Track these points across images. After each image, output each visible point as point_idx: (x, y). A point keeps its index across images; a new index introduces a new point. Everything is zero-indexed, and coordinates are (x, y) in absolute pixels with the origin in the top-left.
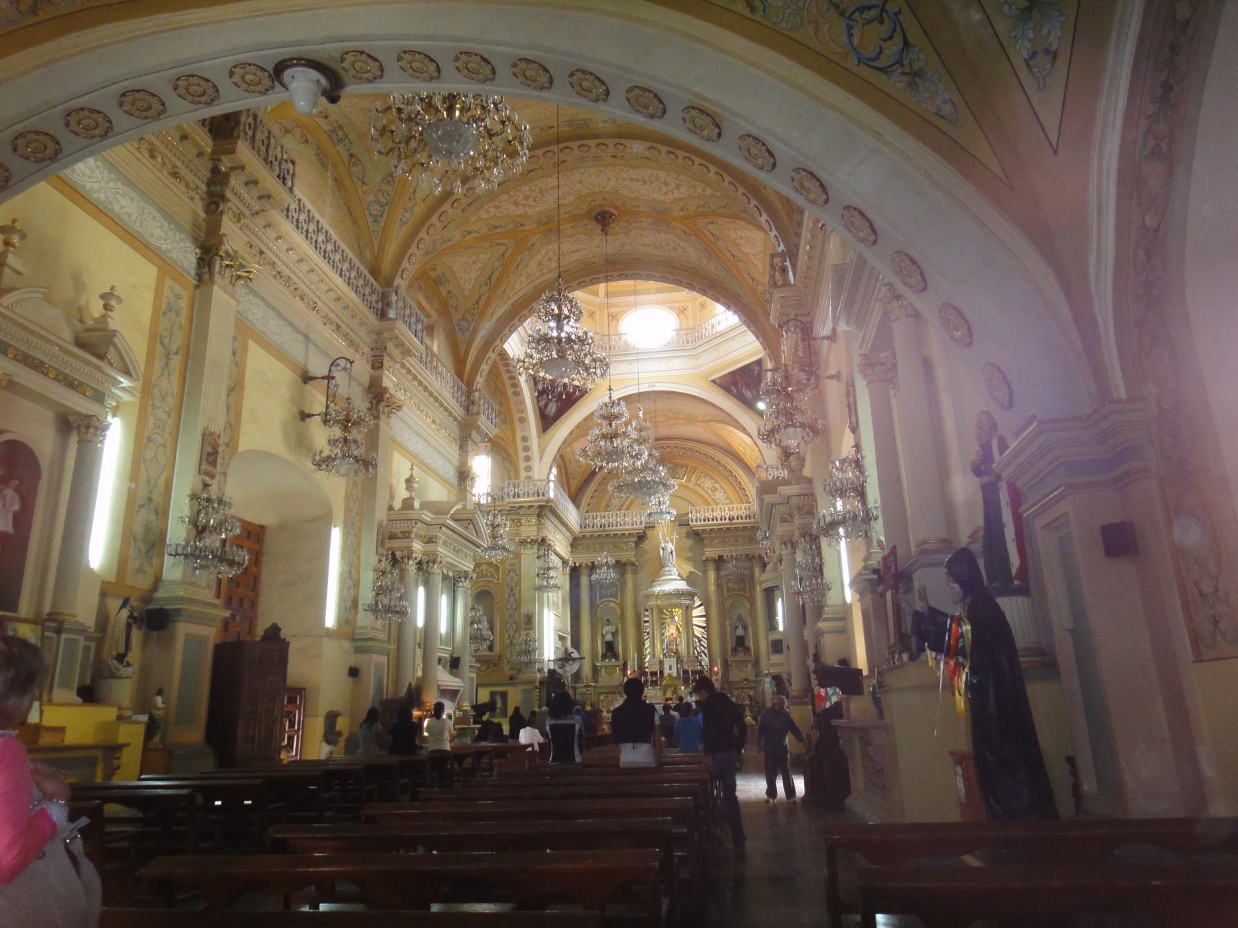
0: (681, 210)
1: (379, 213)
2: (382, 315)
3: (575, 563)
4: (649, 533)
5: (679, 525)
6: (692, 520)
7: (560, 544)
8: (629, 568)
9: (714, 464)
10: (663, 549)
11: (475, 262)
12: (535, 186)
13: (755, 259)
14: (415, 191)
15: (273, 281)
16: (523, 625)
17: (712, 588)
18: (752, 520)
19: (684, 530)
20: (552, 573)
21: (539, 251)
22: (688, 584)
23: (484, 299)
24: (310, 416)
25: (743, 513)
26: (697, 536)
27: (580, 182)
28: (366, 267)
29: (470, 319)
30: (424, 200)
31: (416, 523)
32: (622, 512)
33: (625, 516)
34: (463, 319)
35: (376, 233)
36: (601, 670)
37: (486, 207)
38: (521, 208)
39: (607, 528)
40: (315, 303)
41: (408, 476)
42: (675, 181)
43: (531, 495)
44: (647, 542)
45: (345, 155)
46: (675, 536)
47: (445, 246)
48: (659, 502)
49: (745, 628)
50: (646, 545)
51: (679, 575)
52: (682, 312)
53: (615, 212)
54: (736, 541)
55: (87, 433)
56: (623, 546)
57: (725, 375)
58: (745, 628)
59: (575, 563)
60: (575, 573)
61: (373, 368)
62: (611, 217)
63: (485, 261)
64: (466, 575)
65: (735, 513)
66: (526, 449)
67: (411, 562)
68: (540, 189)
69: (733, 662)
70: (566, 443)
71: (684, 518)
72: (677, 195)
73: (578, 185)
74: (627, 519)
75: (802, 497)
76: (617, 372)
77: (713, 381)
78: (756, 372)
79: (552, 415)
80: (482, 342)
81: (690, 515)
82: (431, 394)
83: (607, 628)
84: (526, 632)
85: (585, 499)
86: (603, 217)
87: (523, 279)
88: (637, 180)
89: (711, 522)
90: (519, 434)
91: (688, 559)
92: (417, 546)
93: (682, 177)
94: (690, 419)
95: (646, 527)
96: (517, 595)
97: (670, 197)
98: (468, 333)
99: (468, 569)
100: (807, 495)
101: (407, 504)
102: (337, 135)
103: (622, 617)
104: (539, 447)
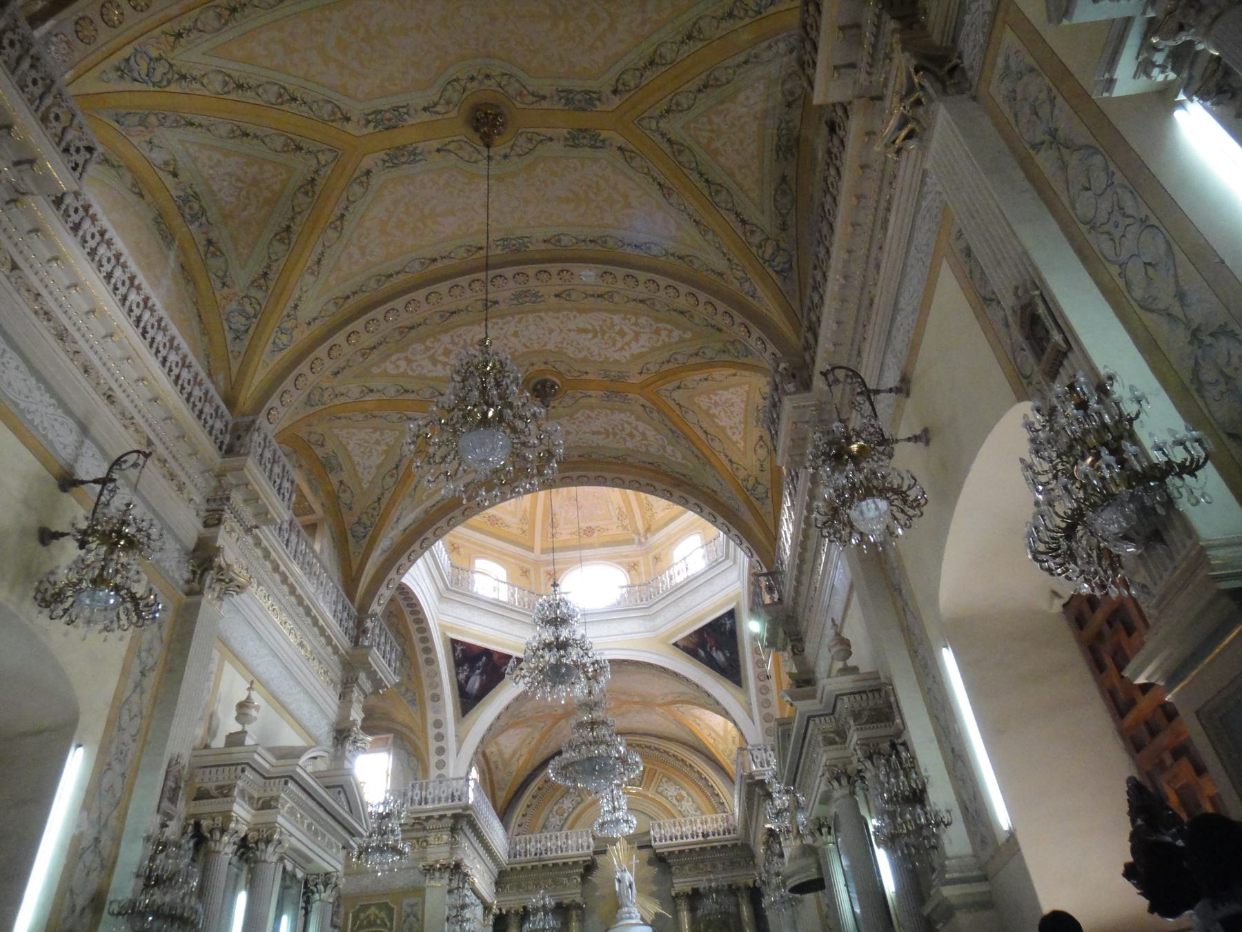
0: (641, 373)
1: (243, 328)
2: (229, 451)
3: (500, 910)
4: (600, 860)
5: (640, 848)
6: (655, 841)
7: (481, 877)
9: (678, 764)
10: (619, 881)
11: (378, 443)
12: (460, 336)
13: (734, 434)
14: (296, 306)
15: (33, 316)
18: (733, 835)
19: (646, 853)
20: (467, 914)
24: (58, 535)
25: (721, 825)
26: (662, 862)
27: (515, 334)
28: (219, 394)
29: (368, 523)
30: (309, 324)
31: (243, 771)
32: (564, 832)
33: (567, 838)
34: (358, 523)
35: (236, 354)
37: (394, 358)
38: (439, 367)
39: (544, 856)
40: (110, 389)
41: (243, 698)
42: (633, 327)
43: (443, 800)
44: (596, 873)
45: (201, 240)
46: (634, 861)
47: (336, 401)
48: (614, 808)
50: (596, 877)
51: (642, 919)
52: (632, 568)
53: (558, 381)
59: (500, 910)
61: (206, 525)
62: (552, 387)
63: (392, 443)
64: (327, 880)
65: (710, 827)
66: (440, 737)
67: (226, 838)
68: (465, 340)
70: (493, 732)
71: (646, 838)
72: (636, 349)
73: (514, 340)
74: (570, 842)
75: (858, 697)
77: (675, 644)
78: (728, 626)
80: (383, 557)
81: (652, 833)
82: (300, 602)
85: (516, 818)
86: (544, 386)
88: (585, 331)
89: (680, 841)
90: (431, 717)
91: (653, 895)
92: (242, 813)
93: (642, 320)
94: (646, 703)
95: (596, 853)
97: (627, 354)
98: (364, 543)
99: (331, 869)
100: (864, 692)
101: (235, 740)
102: (191, 208)
104: (456, 736)
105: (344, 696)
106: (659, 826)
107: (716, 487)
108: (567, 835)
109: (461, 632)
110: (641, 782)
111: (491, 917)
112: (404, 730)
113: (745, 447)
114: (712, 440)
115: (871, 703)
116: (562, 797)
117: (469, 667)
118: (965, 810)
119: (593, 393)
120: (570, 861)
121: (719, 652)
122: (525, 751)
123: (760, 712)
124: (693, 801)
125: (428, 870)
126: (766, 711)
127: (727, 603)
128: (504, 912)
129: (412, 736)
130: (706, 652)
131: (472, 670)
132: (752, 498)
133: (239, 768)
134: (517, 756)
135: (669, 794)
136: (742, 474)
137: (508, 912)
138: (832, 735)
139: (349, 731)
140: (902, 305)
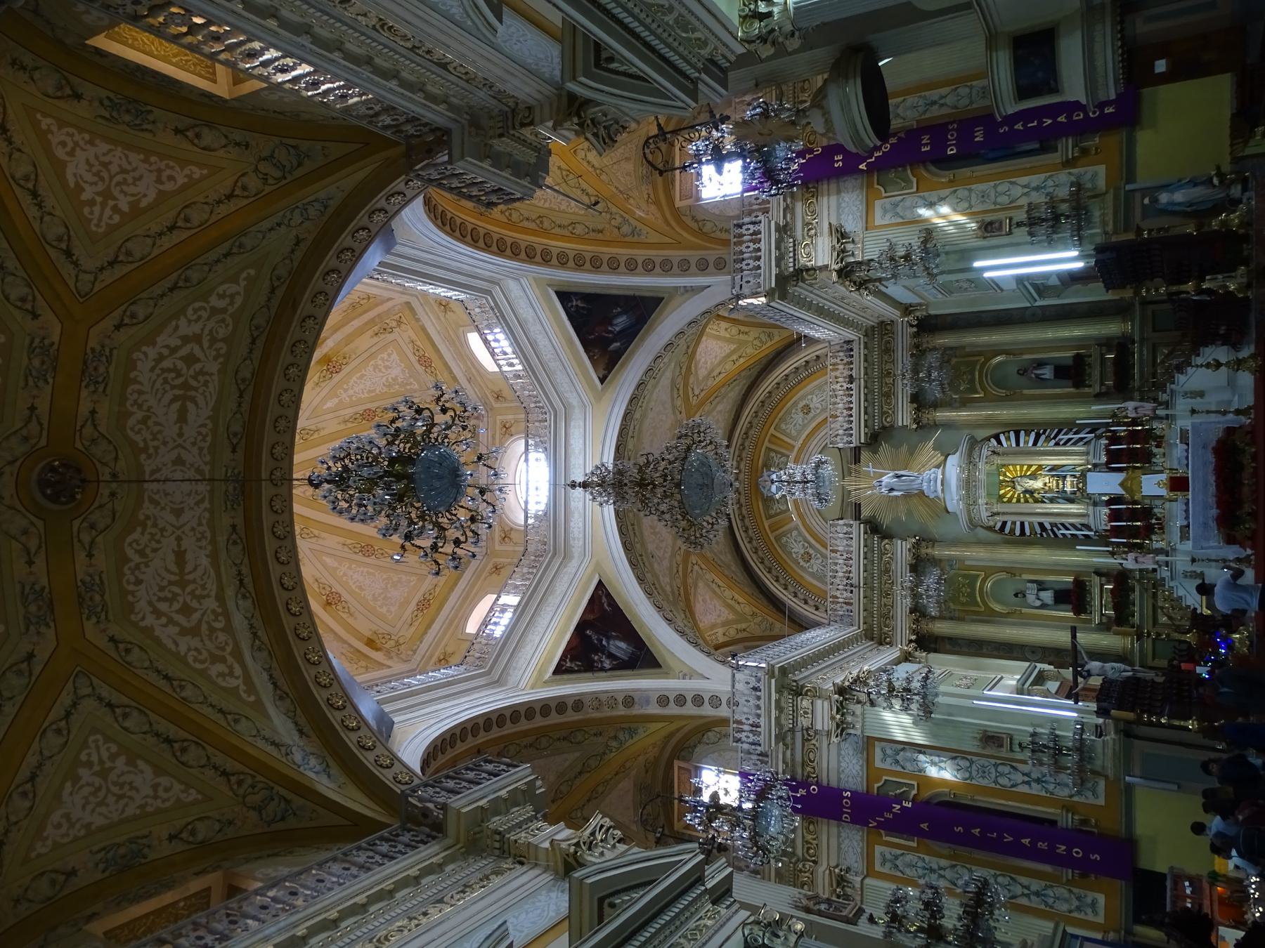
3: (911, 641)
6: (851, 442)
8: (923, 551)
10: (892, 490)
16: (1004, 753)
17: (963, 415)
19: (865, 455)
21: (148, 631)
22: (954, 454)
23: (219, 759)
33: (836, 551)
34: (259, 809)
49: (1041, 364)
50: (886, 520)
51: (938, 467)
52: (507, 430)
56: (885, 558)
59: (911, 641)
60: (927, 643)
62: (53, 470)
66: (681, 700)
69: (1102, 384)
74: (840, 548)
76: (581, 535)
77: (602, 380)
79: (631, 649)
81: (840, 445)
83: (1031, 598)
84: (1017, 748)
85: (807, 611)
90: (654, 709)
91: (912, 452)
95: (857, 517)
98: (298, 801)
103: (1011, 571)
105: (523, 857)
108: (832, 551)
109: (549, 661)
110: (783, 455)
111: (917, 654)
112: (669, 748)
119: (84, 409)
121: (615, 322)
122: (728, 593)
123: (695, 275)
125: (842, 731)
126: (693, 268)
127: (548, 299)
128: (913, 637)
129: (679, 736)
130: (614, 341)
131: (602, 649)
135: (800, 422)
137: (914, 632)
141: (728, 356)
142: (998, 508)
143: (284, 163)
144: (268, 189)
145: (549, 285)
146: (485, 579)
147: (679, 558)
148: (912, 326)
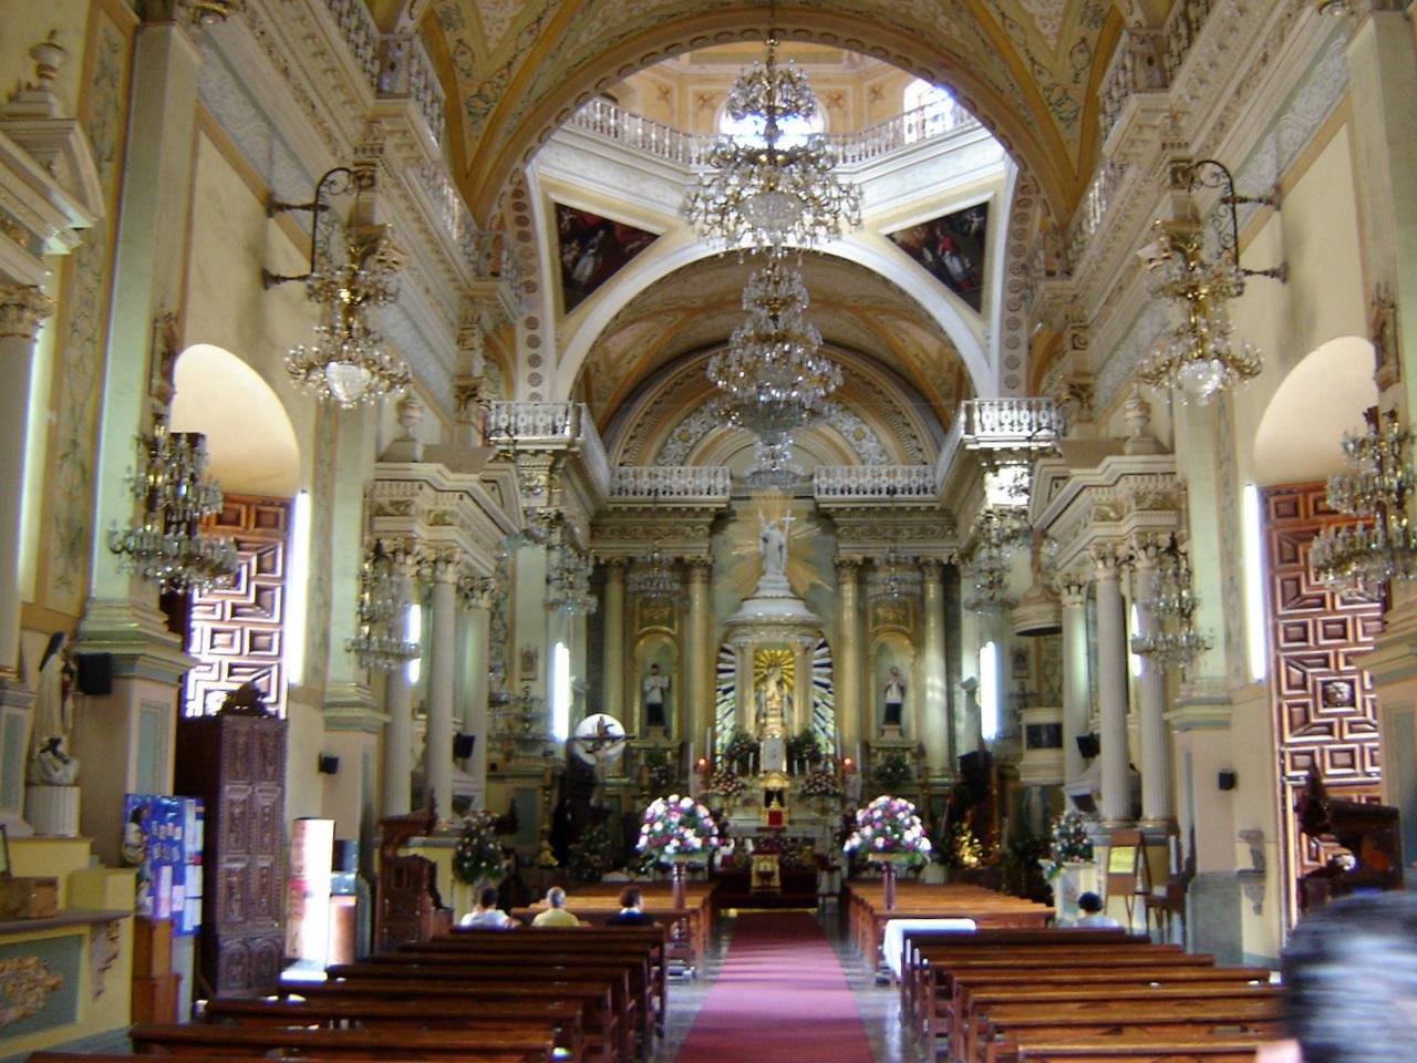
6: (819, 490)
10: (766, 540)
13: (1045, 26)
18: (929, 496)
22: (807, 607)
23: (522, 57)
24: (279, 279)
26: (824, 517)
29: (492, 95)
32: (688, 468)
34: (479, 95)
36: (637, 756)
39: (661, 497)
49: (902, 690)
51: (792, 589)
54: (897, 532)
55: (20, 320)
57: (915, 228)
58: (902, 690)
65: (900, 481)
66: (534, 342)
69: (879, 749)
70: (606, 334)
71: (806, 484)
75: (1146, 477)
77: (890, 237)
79: (584, 279)
81: (815, 481)
83: (650, 682)
85: (621, 444)
87: (596, 24)
92: (421, 530)
95: (733, 498)
96: (507, 617)
98: (484, 123)
103: (681, 664)
104: (557, 340)
106: (828, 471)
107: (1005, 86)
113: (1057, 45)
114: (1011, 27)
115: (1160, 486)
116: (688, 417)
117: (579, 245)
118: (1228, 637)
120: (698, 507)
122: (640, 352)
123: (1001, 354)
124: (879, 442)
127: (983, 189)
128: (602, 562)
131: (583, 251)
132: (1053, 115)
133: (417, 484)
134: (629, 357)
135: (845, 428)
136: (1044, 80)
138: (1107, 509)
139: (474, 389)
140: (1299, 103)
141: (924, 351)
142: (749, 653)
143: (1063, 107)
144: (1040, 91)
145: (995, 195)
146: (654, 81)
147: (682, 303)
148: (950, 557)
